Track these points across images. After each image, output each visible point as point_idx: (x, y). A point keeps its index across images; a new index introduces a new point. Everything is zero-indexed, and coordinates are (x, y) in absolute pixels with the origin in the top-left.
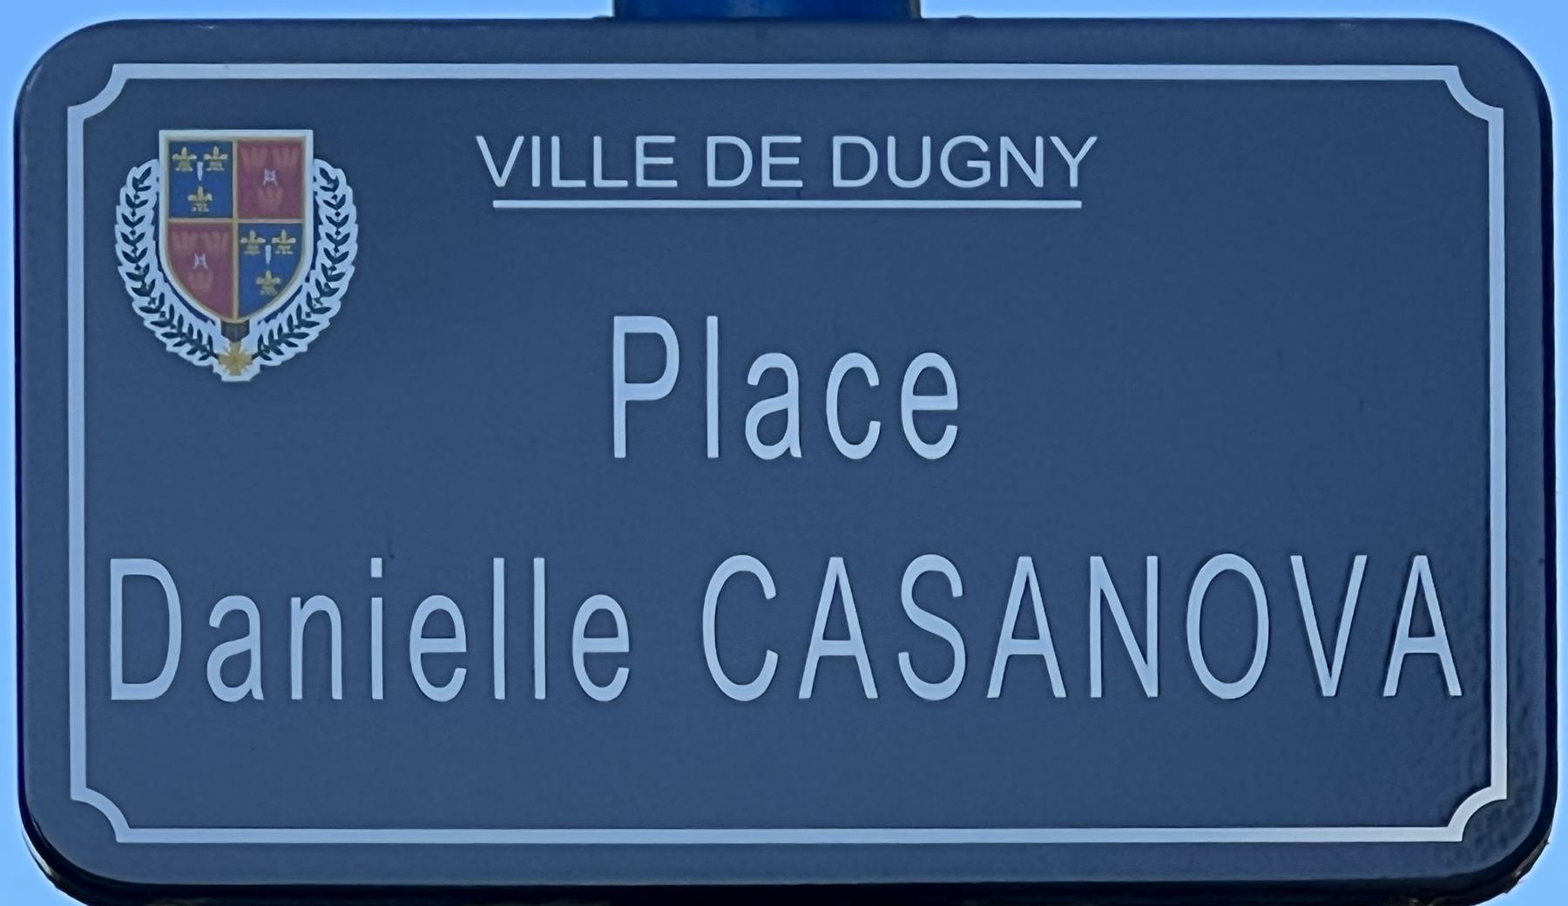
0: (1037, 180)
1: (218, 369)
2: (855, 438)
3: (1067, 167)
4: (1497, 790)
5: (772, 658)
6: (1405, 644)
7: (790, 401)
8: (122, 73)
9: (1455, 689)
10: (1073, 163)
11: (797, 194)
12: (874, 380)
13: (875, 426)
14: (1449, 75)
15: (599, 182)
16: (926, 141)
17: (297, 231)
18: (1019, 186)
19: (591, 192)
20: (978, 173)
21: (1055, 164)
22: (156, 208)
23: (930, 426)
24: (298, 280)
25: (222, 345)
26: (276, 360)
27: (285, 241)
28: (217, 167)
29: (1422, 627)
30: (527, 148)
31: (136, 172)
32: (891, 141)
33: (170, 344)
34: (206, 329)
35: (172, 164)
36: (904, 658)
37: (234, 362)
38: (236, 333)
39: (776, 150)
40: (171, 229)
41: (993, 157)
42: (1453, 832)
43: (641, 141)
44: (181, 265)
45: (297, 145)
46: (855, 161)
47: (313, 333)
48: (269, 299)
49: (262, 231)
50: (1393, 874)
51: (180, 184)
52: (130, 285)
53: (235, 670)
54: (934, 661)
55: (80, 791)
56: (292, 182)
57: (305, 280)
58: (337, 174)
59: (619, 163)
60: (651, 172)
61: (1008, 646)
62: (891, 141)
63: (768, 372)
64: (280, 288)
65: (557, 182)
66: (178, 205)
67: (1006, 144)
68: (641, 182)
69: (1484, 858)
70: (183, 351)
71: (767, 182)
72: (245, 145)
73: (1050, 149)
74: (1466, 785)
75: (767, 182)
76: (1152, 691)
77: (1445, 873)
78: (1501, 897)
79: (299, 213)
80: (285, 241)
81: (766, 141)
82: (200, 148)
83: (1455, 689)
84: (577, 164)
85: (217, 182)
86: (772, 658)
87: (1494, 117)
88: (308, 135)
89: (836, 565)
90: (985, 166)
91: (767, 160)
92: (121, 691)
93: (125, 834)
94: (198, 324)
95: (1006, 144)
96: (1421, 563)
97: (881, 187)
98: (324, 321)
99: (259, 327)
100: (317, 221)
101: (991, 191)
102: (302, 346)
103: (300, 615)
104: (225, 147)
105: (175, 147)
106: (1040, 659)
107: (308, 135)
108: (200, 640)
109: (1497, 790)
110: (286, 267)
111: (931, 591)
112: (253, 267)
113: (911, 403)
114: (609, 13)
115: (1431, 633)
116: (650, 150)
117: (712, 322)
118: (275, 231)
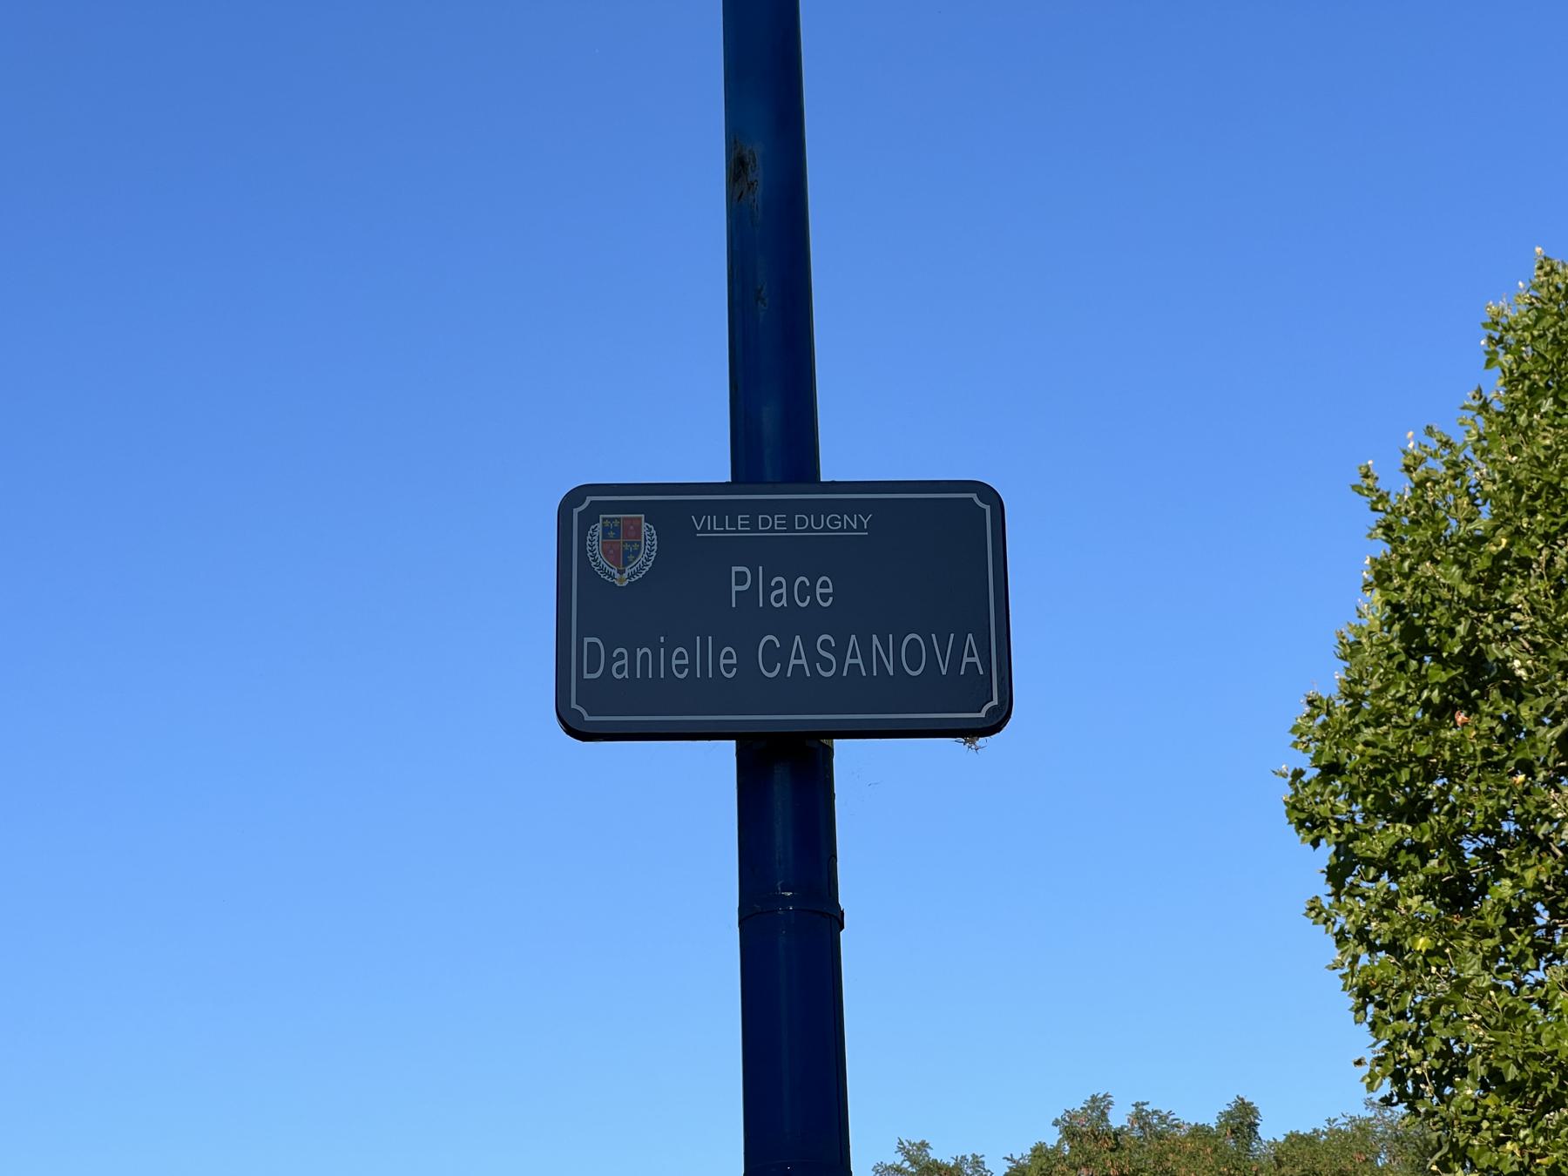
0: (855, 527)
1: (616, 582)
2: (803, 601)
3: (863, 523)
4: (995, 702)
5: (779, 665)
6: (966, 659)
7: (783, 590)
8: (589, 499)
9: (981, 673)
10: (865, 522)
11: (785, 531)
12: (808, 584)
13: (808, 598)
14: (974, 496)
15: (727, 529)
16: (822, 516)
17: (639, 543)
18: (850, 529)
19: (725, 531)
20: (838, 525)
21: (860, 523)
22: (599, 537)
23: (825, 597)
24: (640, 557)
25: (617, 576)
26: (633, 580)
27: (636, 546)
28: (616, 525)
29: (971, 654)
30: (706, 519)
31: (593, 527)
32: (812, 516)
33: (602, 575)
34: (613, 571)
35: (603, 525)
36: (818, 665)
37: (621, 581)
38: (621, 572)
39: (778, 519)
40: (602, 542)
41: (842, 520)
42: (982, 715)
43: (739, 517)
44: (606, 553)
45: (640, 519)
46: (802, 522)
47: (644, 572)
48: (631, 562)
49: (629, 543)
50: (965, 727)
51: (606, 530)
52: (591, 559)
53: (620, 669)
54: (827, 665)
55: (574, 705)
56: (639, 529)
57: (641, 557)
58: (651, 527)
59: (733, 523)
60: (742, 526)
61: (849, 661)
62: (812, 516)
63: (777, 582)
64: (634, 559)
65: (715, 529)
66: (605, 536)
67: (845, 516)
68: (740, 528)
69: (992, 722)
70: (606, 578)
71: (776, 528)
72: (625, 519)
73: (858, 517)
74: (985, 701)
75: (776, 528)
76: (891, 674)
77: (980, 727)
78: (997, 735)
79: (640, 537)
80: (636, 546)
81: (776, 516)
82: (611, 520)
83: (981, 673)
84: (721, 523)
85: (617, 530)
86: (779, 665)
87: (988, 508)
88: (643, 516)
89: (798, 638)
90: (840, 523)
91: (776, 522)
92: (587, 676)
93: (587, 718)
94: (610, 570)
95: (845, 516)
96: (970, 636)
97: (810, 529)
98: (647, 568)
99: (628, 571)
100: (645, 540)
101: (842, 530)
102: (641, 576)
103: (639, 653)
104: (619, 519)
105: (604, 519)
106: (858, 665)
107: (643, 516)
108: (610, 661)
109: (995, 702)
110: (636, 553)
111: (825, 644)
112: (626, 553)
113: (819, 591)
114: (730, 480)
115: (974, 656)
116: (742, 519)
117: (761, 568)
118: (633, 543)
